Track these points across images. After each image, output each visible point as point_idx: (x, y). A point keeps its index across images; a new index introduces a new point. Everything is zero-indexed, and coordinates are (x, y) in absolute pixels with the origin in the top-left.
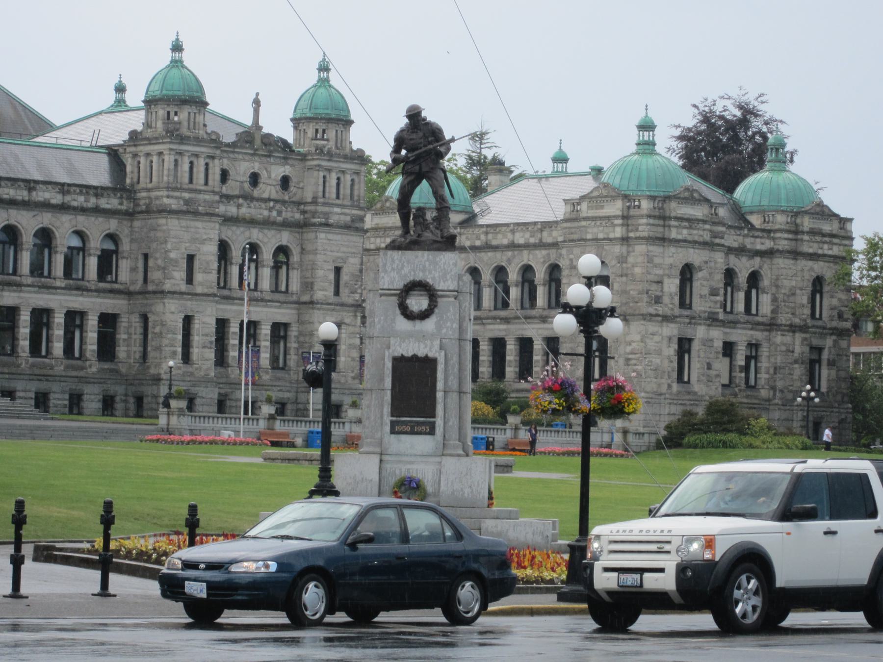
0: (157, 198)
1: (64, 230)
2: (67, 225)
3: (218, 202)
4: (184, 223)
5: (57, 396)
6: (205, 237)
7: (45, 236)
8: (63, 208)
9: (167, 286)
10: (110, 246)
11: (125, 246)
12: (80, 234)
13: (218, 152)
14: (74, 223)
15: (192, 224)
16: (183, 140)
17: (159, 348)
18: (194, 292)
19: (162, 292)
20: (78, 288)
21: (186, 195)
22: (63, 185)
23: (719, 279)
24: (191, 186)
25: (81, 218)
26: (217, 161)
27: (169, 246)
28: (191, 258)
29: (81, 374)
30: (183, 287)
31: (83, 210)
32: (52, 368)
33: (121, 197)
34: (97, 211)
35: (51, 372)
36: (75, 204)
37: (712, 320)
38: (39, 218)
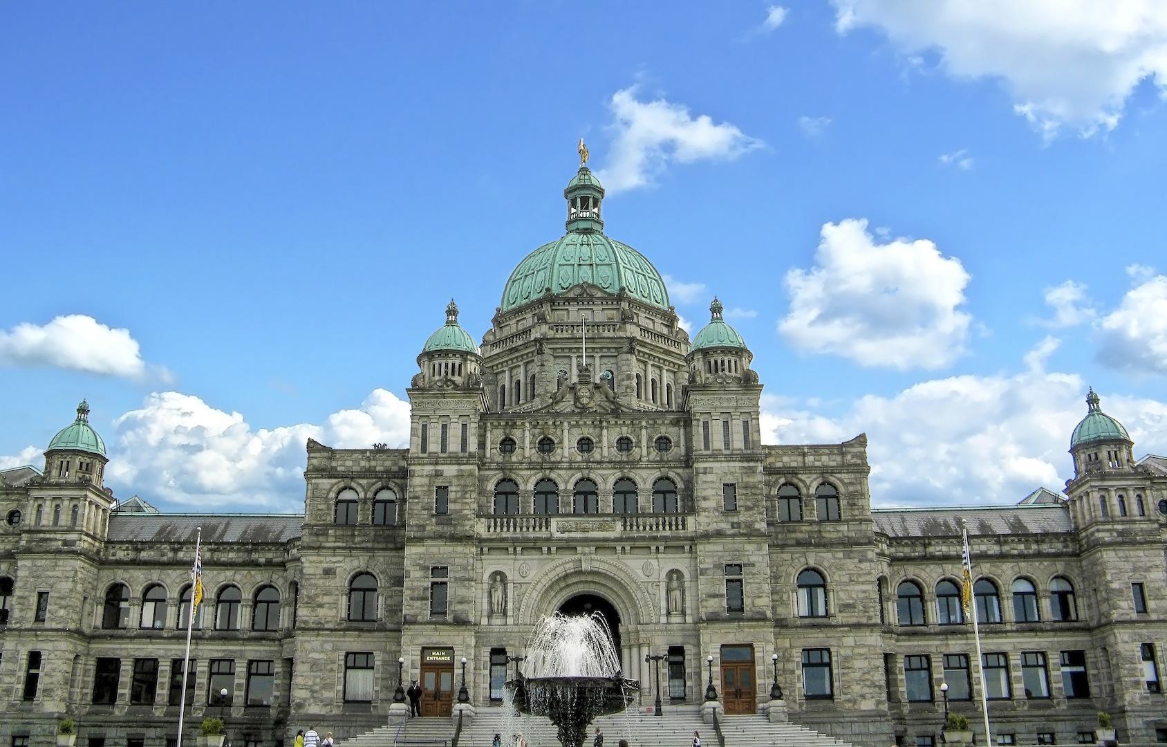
0: (1093, 534)
1: (1006, 574)
2: (1009, 572)
3: (1158, 530)
4: (1121, 554)
5: (1022, 736)
6: (1149, 564)
8: (1002, 557)
9: (1115, 616)
10: (1064, 586)
11: (1079, 585)
12: (1026, 578)
13: (1148, 483)
14: (1016, 569)
15: (1132, 553)
16: (1104, 477)
17: (1119, 679)
18: (1148, 618)
19: (1109, 623)
20: (1032, 630)
21: (1120, 527)
22: (999, 536)
24: (1124, 518)
25: (1023, 565)
26: (1148, 492)
27: (1109, 578)
28: (1139, 587)
29: (1047, 712)
30: (1134, 616)
31: (1022, 556)
32: (1014, 709)
33: (1065, 541)
34: (1039, 555)
35: (1013, 713)
36: (1015, 552)
38: (978, 569)
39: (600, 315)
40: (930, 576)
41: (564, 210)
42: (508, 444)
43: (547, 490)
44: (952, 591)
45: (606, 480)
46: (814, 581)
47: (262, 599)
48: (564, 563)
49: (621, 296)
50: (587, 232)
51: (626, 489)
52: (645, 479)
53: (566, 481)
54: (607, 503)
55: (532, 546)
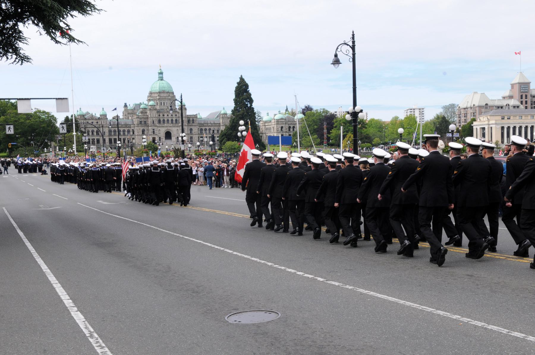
1: (212, 128)
7: (210, 129)
23: (287, 128)
37: (286, 132)
39: (165, 95)
40: (204, 128)
41: (157, 76)
42: (159, 115)
43: (164, 120)
44: (206, 130)
45: (170, 119)
46: (191, 130)
47: (129, 131)
48: (166, 128)
49: (168, 92)
50: (162, 80)
51: (172, 120)
52: (174, 119)
53: (166, 120)
54: (170, 122)
55: (163, 127)
